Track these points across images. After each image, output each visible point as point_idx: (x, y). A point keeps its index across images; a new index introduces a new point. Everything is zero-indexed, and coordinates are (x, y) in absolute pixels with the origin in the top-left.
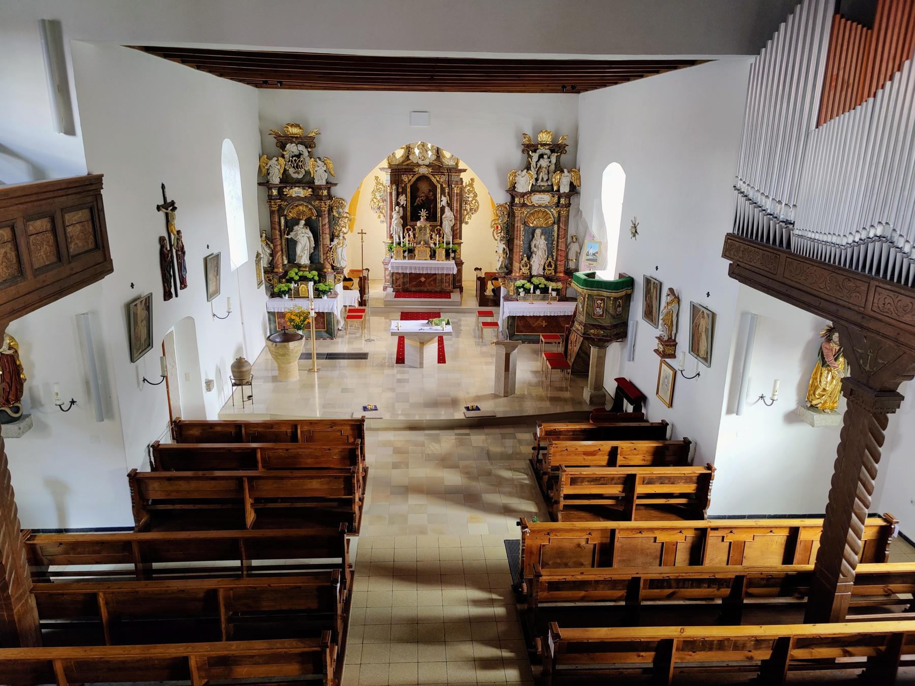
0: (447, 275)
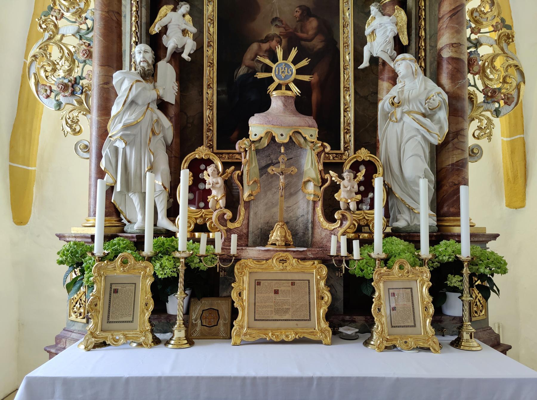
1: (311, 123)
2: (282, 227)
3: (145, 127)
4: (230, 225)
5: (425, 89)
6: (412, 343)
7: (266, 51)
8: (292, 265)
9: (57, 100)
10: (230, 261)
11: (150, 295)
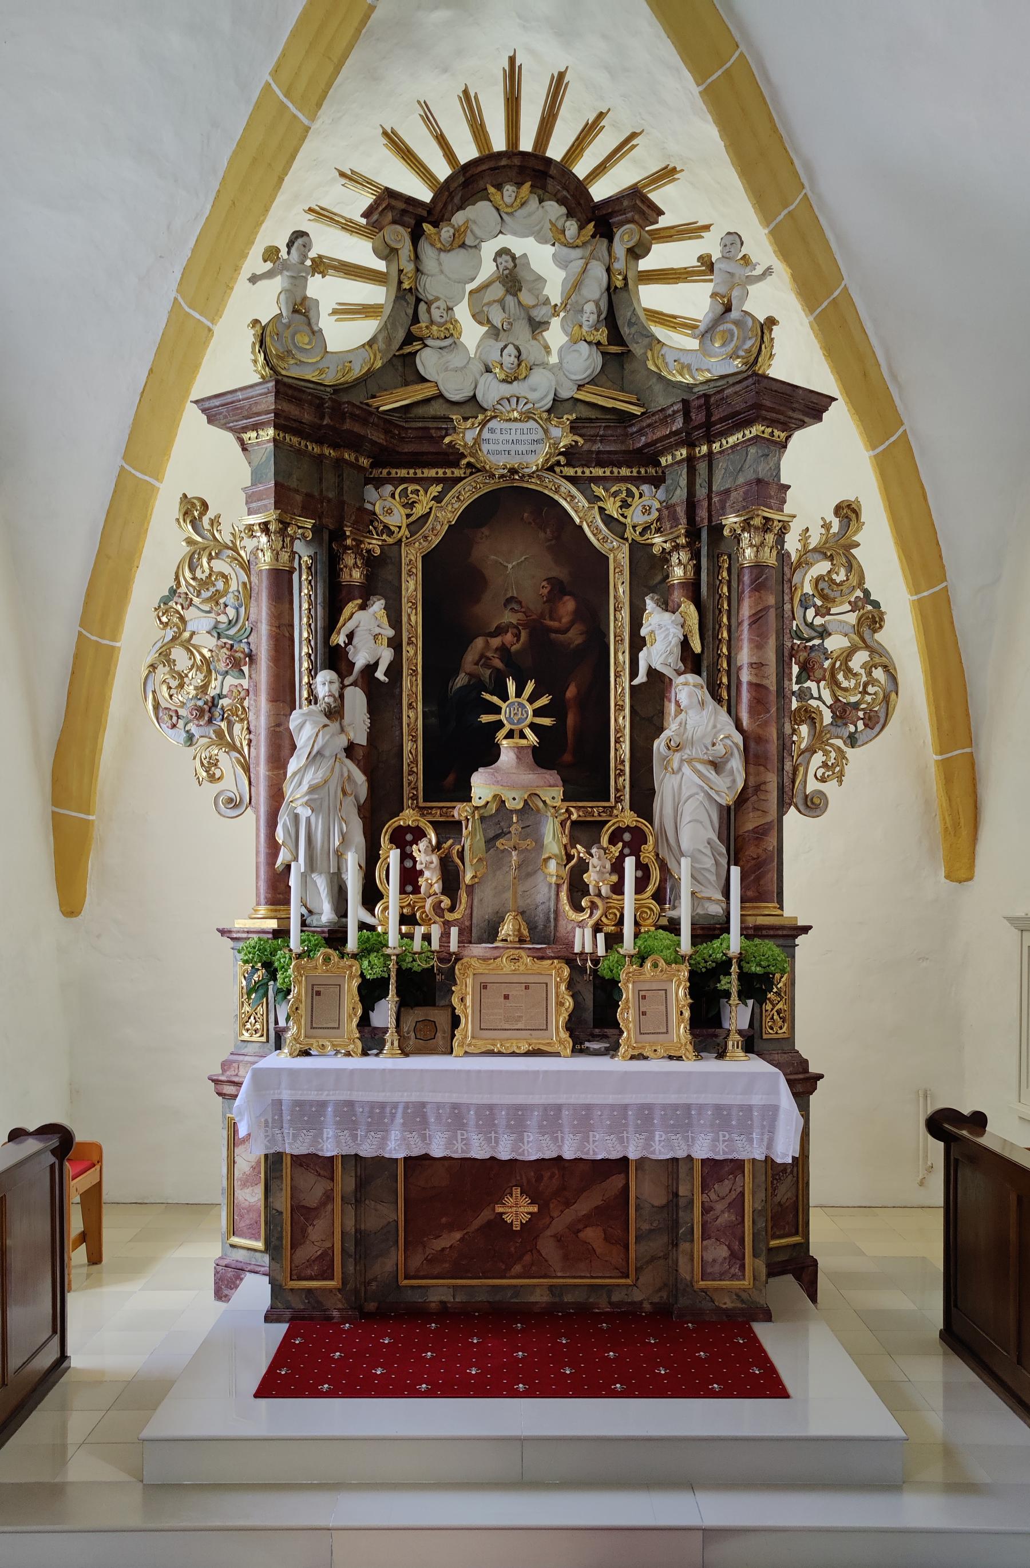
0: (716, 1170)
1: (552, 782)
2: (515, 918)
3: (334, 785)
4: (449, 916)
5: (715, 727)
6: (661, 1052)
7: (497, 649)
8: (526, 965)
9: (187, 732)
10: (449, 960)
11: (357, 999)
